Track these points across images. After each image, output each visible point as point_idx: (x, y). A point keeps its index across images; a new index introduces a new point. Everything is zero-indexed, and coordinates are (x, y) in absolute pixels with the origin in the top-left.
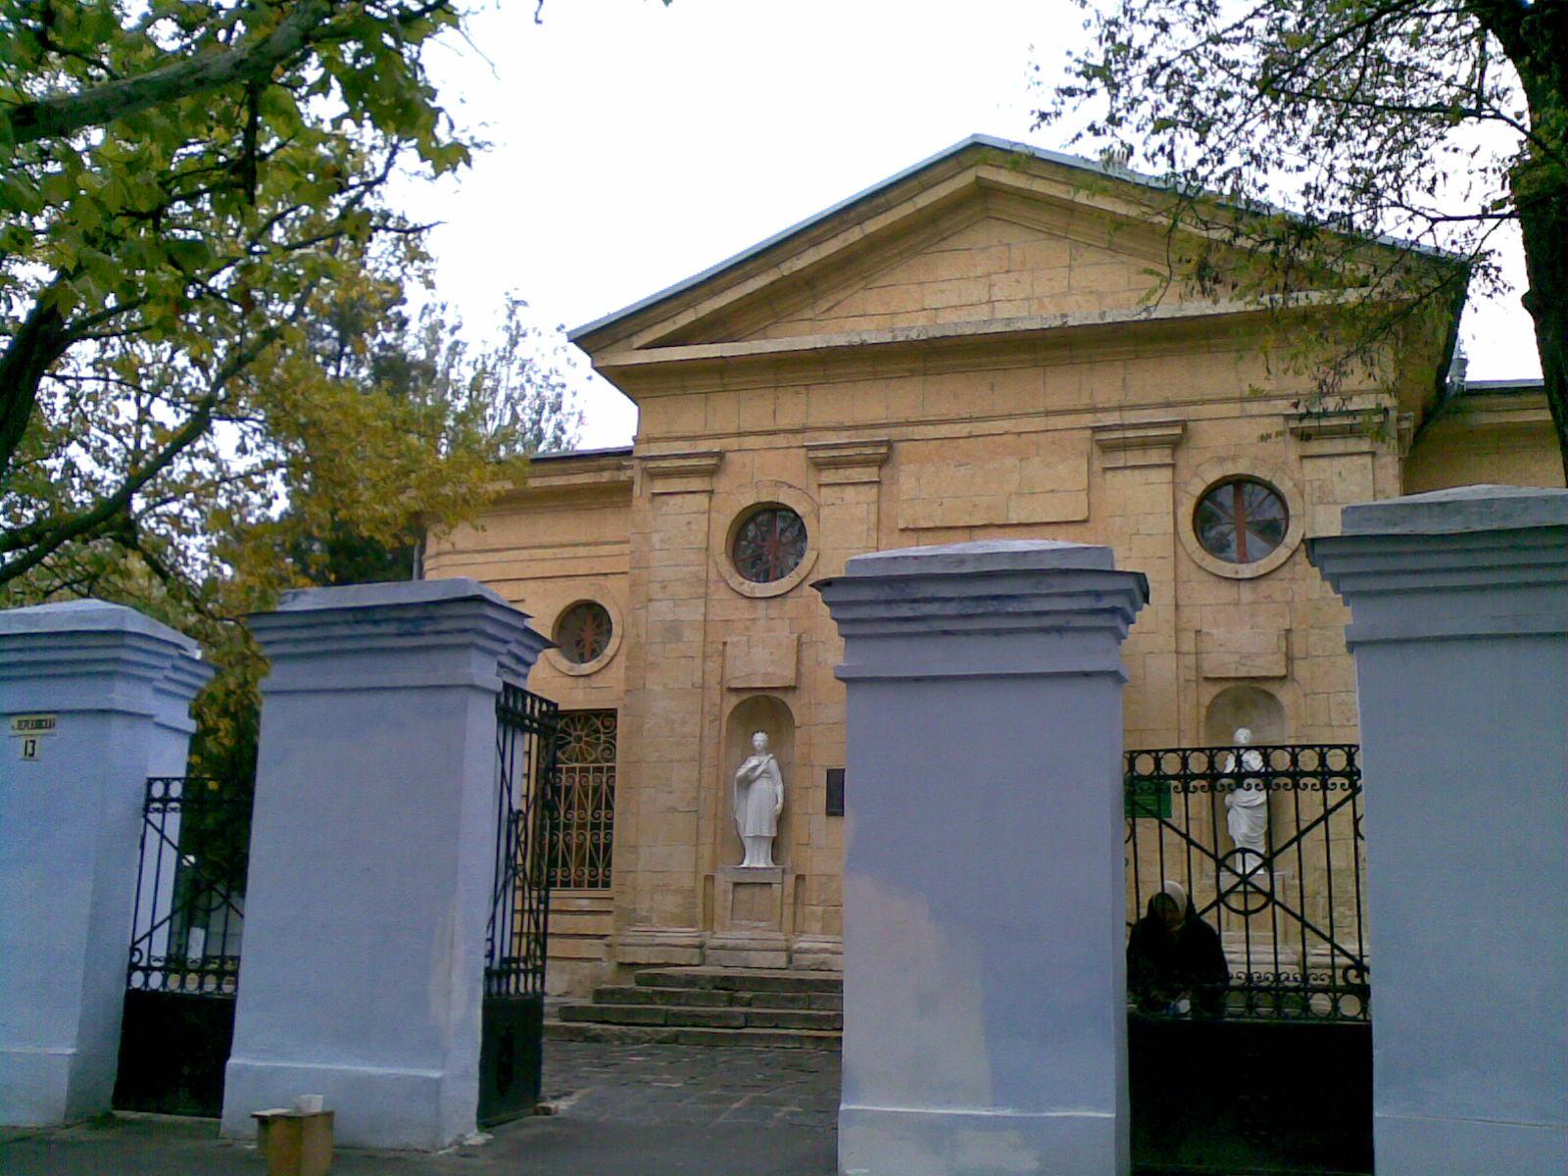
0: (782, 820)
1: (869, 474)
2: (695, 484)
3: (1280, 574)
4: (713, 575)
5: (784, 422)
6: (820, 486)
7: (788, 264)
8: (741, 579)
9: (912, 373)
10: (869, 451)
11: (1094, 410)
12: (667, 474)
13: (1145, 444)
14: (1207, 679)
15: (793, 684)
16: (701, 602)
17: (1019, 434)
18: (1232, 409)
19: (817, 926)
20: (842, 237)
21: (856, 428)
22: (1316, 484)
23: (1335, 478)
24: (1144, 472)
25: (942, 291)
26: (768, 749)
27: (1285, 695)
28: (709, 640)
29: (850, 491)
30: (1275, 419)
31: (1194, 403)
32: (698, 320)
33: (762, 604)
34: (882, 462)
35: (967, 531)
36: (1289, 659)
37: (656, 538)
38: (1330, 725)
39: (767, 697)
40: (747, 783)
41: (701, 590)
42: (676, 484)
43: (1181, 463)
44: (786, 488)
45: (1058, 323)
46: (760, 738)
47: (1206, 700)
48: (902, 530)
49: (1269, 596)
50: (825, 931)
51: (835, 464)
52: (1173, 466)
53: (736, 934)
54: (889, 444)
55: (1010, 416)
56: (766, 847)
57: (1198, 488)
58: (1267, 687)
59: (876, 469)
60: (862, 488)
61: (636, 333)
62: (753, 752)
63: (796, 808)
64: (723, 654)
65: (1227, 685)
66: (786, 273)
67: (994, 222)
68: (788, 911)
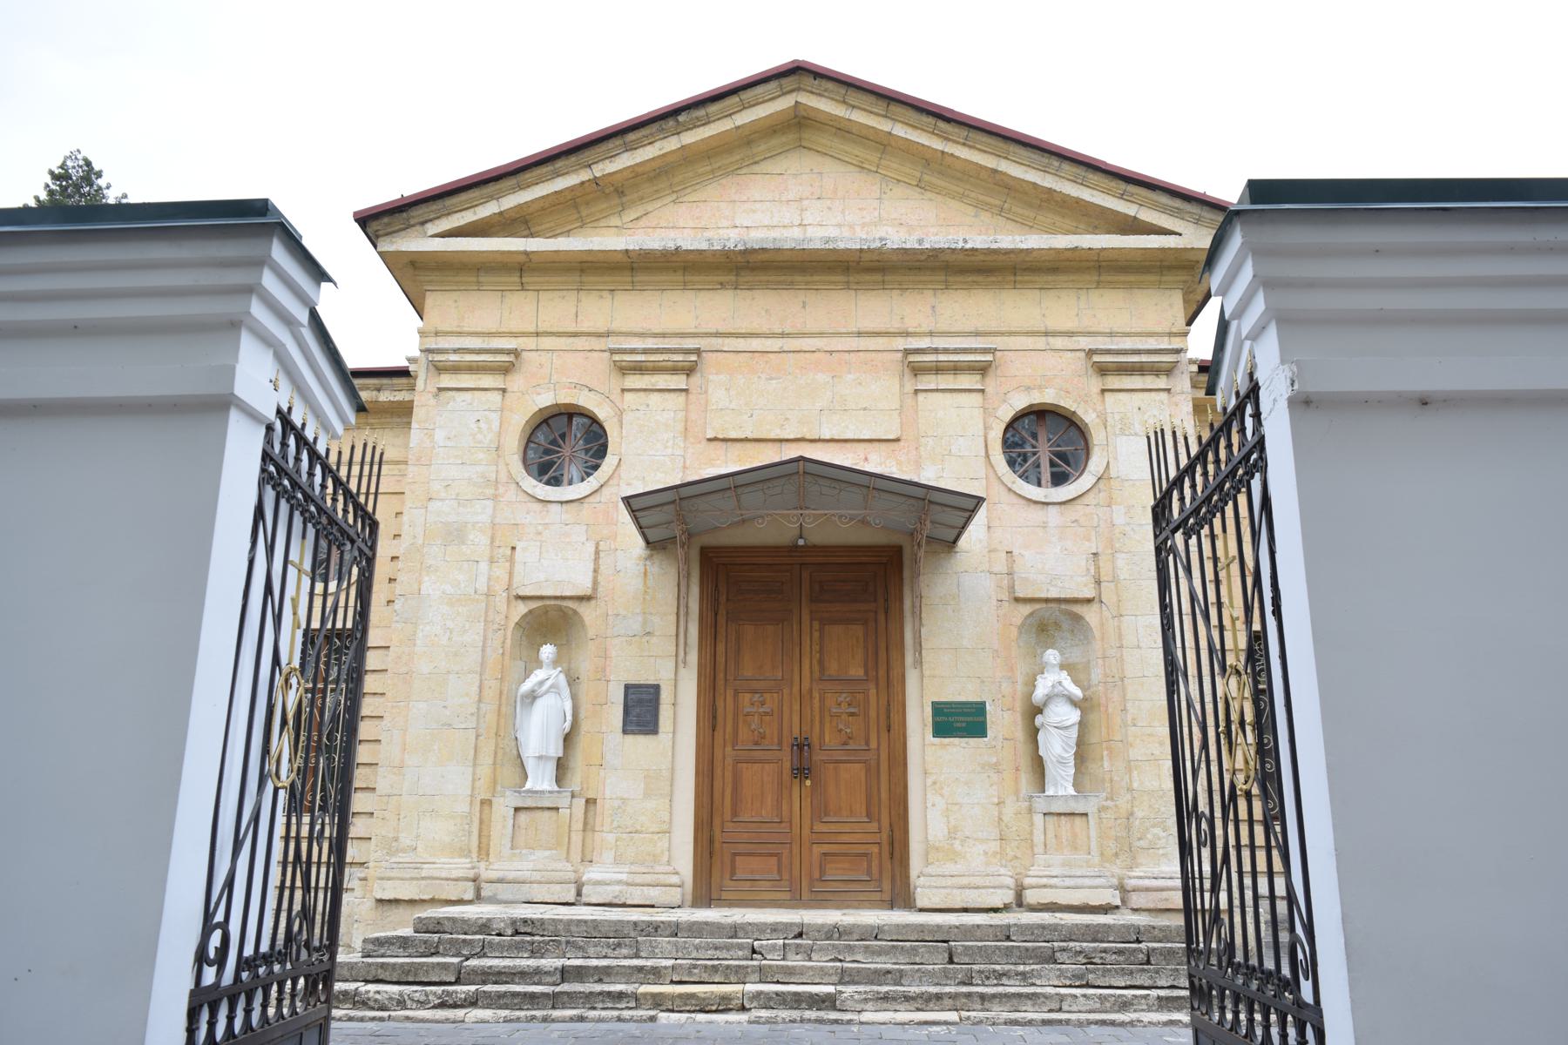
0: (568, 739)
1: (678, 381)
2: (487, 381)
3: (1085, 500)
4: (503, 477)
5: (585, 326)
6: (623, 390)
7: (600, 166)
8: (534, 482)
9: (723, 286)
10: (680, 357)
11: (907, 334)
12: (456, 369)
13: (956, 369)
14: (1017, 600)
15: (589, 592)
16: (489, 503)
17: (831, 352)
18: (1040, 342)
19: (608, 856)
20: (658, 145)
21: (664, 335)
22: (1117, 417)
23: (1136, 410)
24: (955, 395)
25: (754, 211)
26: (556, 663)
27: (1091, 615)
28: (497, 543)
29: (655, 398)
30: (1078, 354)
31: (1002, 334)
32: (501, 213)
33: (555, 508)
34: (689, 371)
35: (778, 445)
36: (1098, 582)
37: (439, 436)
38: (1139, 647)
39: (560, 609)
40: (532, 697)
41: (490, 491)
42: (466, 380)
43: (989, 390)
44: (587, 390)
45: (877, 244)
46: (547, 651)
47: (1018, 621)
48: (709, 440)
49: (1076, 521)
50: (618, 861)
51: (639, 369)
52: (982, 391)
53: (516, 865)
54: (698, 352)
55: (821, 334)
56: (551, 768)
57: (1007, 414)
58: (1077, 609)
59: (684, 377)
60: (667, 395)
61: (431, 220)
62: (539, 664)
63: (585, 726)
64: (511, 560)
65: (1038, 606)
66: (598, 175)
67: (802, 150)
68: (577, 838)
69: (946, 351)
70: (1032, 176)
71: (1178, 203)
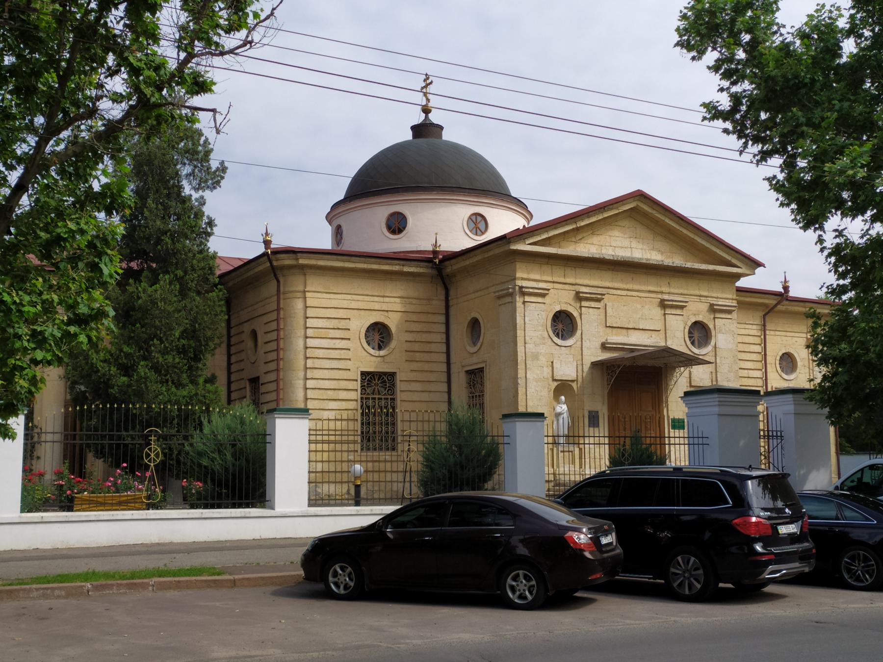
33: (563, 348)
45: (661, 263)
69: (676, 301)
70: (704, 243)
71: (743, 258)
